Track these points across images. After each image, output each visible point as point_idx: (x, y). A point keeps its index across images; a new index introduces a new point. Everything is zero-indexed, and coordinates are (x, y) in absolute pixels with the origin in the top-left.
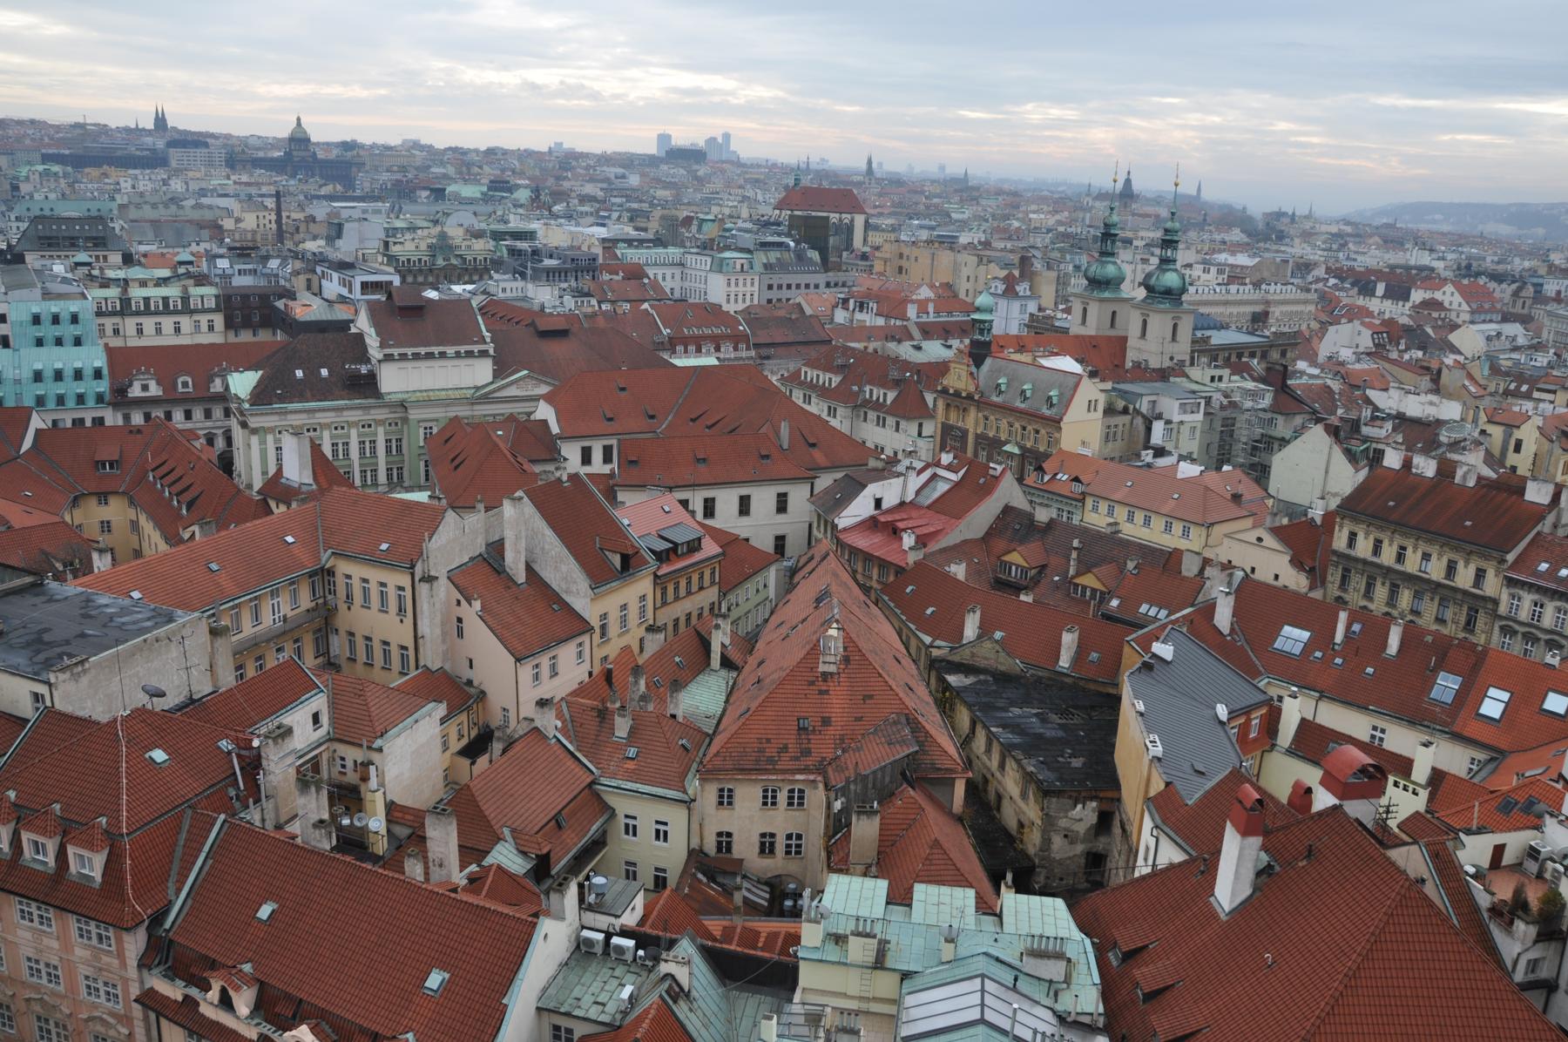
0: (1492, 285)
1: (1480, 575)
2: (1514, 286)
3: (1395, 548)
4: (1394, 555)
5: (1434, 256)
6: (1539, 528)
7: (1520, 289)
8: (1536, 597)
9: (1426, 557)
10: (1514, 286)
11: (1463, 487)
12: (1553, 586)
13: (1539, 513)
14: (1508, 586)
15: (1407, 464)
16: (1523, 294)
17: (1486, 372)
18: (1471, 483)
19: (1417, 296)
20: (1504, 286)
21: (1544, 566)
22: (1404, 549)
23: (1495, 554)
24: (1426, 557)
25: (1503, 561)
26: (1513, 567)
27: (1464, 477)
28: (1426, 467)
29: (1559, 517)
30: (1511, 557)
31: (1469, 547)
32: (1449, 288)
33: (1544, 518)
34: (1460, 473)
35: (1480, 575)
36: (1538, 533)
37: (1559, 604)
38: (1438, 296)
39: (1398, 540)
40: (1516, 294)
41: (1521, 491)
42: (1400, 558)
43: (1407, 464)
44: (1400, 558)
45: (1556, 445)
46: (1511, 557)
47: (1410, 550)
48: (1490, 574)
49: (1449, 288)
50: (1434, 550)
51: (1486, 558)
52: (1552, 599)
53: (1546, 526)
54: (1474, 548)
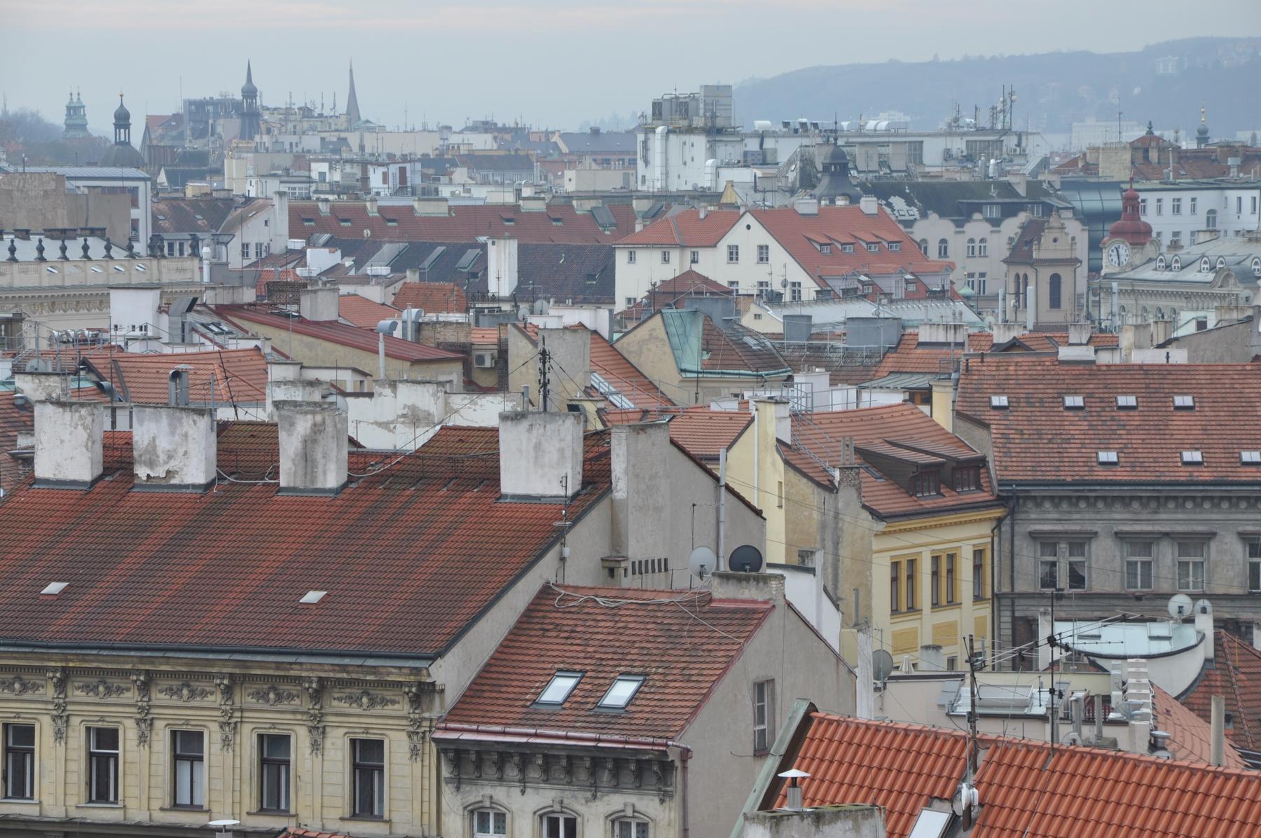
0: (933, 229)
1: (367, 758)
2: (1012, 226)
3: (77, 738)
4: (79, 765)
5: (729, 151)
6: (544, 571)
7: (1031, 234)
8: (542, 797)
9: (187, 747)
10: (1012, 226)
11: (309, 500)
12: (584, 737)
13: (545, 526)
14: (458, 782)
15: (118, 458)
16: (1046, 249)
17: (693, 360)
18: (332, 476)
19: (636, 275)
20: (977, 228)
21: (559, 689)
22: (106, 738)
23: (394, 671)
24: (187, 747)
25: (424, 692)
26: (458, 712)
27: (307, 458)
28: (180, 452)
29: (616, 535)
30: (452, 673)
31: (312, 669)
32: (748, 235)
33: (558, 536)
34: (289, 446)
35: (367, 758)
36: (546, 591)
37: (616, 802)
38: (713, 265)
39: (87, 708)
40: (1020, 253)
41: (492, 478)
42: (102, 774)
43: (118, 458)
44: (102, 774)
45: (847, 497)
46: (452, 673)
47: (129, 734)
48: (397, 748)
49: (748, 235)
50: (205, 714)
51: (371, 691)
52: (595, 790)
53: (577, 559)
54: (325, 667)
